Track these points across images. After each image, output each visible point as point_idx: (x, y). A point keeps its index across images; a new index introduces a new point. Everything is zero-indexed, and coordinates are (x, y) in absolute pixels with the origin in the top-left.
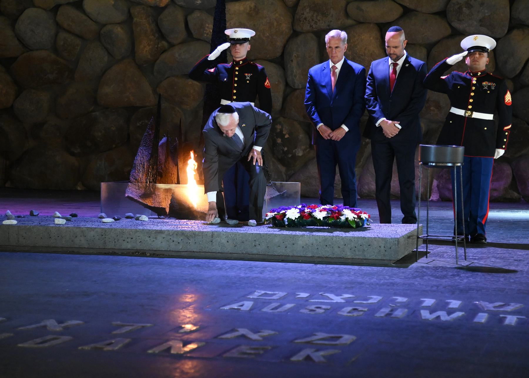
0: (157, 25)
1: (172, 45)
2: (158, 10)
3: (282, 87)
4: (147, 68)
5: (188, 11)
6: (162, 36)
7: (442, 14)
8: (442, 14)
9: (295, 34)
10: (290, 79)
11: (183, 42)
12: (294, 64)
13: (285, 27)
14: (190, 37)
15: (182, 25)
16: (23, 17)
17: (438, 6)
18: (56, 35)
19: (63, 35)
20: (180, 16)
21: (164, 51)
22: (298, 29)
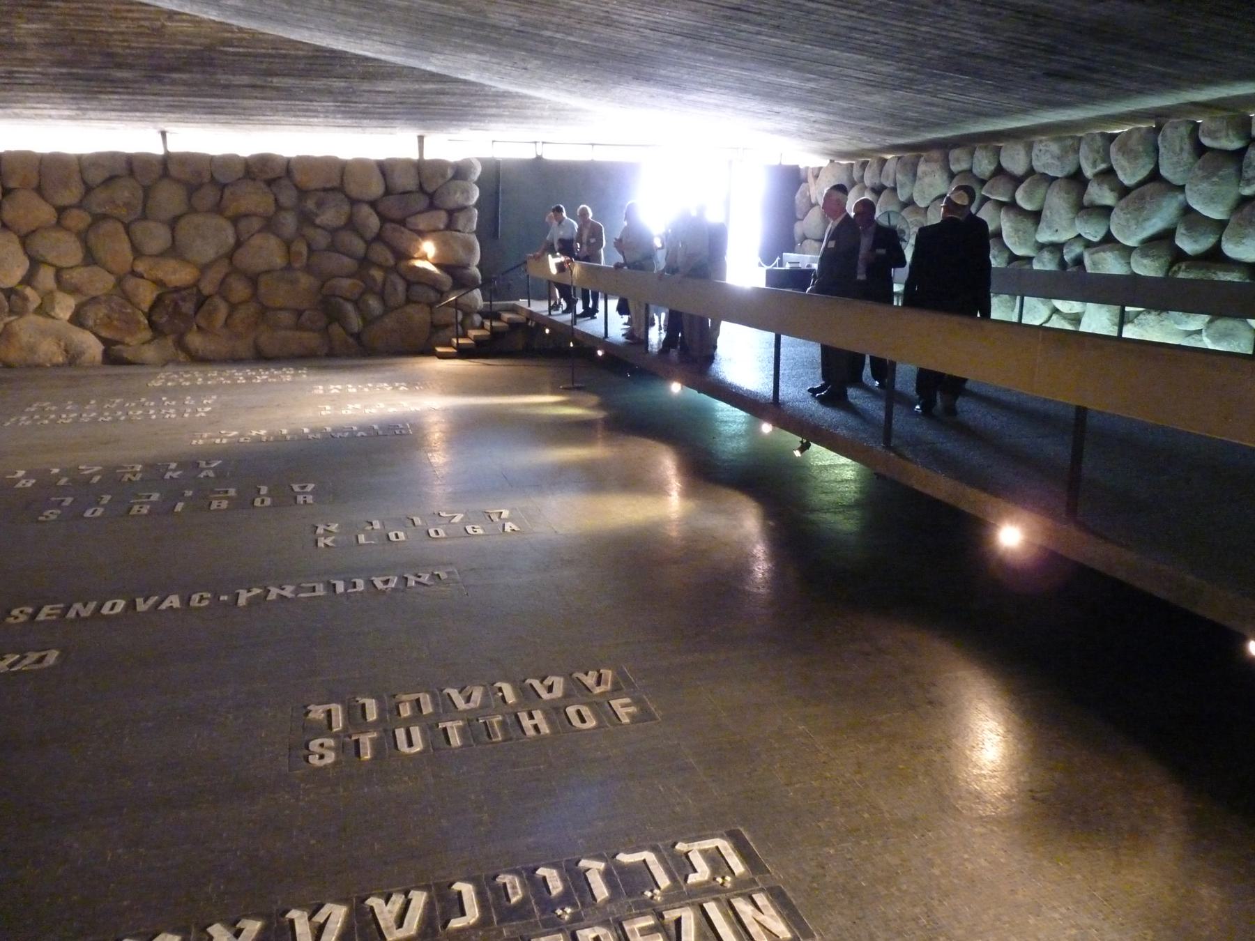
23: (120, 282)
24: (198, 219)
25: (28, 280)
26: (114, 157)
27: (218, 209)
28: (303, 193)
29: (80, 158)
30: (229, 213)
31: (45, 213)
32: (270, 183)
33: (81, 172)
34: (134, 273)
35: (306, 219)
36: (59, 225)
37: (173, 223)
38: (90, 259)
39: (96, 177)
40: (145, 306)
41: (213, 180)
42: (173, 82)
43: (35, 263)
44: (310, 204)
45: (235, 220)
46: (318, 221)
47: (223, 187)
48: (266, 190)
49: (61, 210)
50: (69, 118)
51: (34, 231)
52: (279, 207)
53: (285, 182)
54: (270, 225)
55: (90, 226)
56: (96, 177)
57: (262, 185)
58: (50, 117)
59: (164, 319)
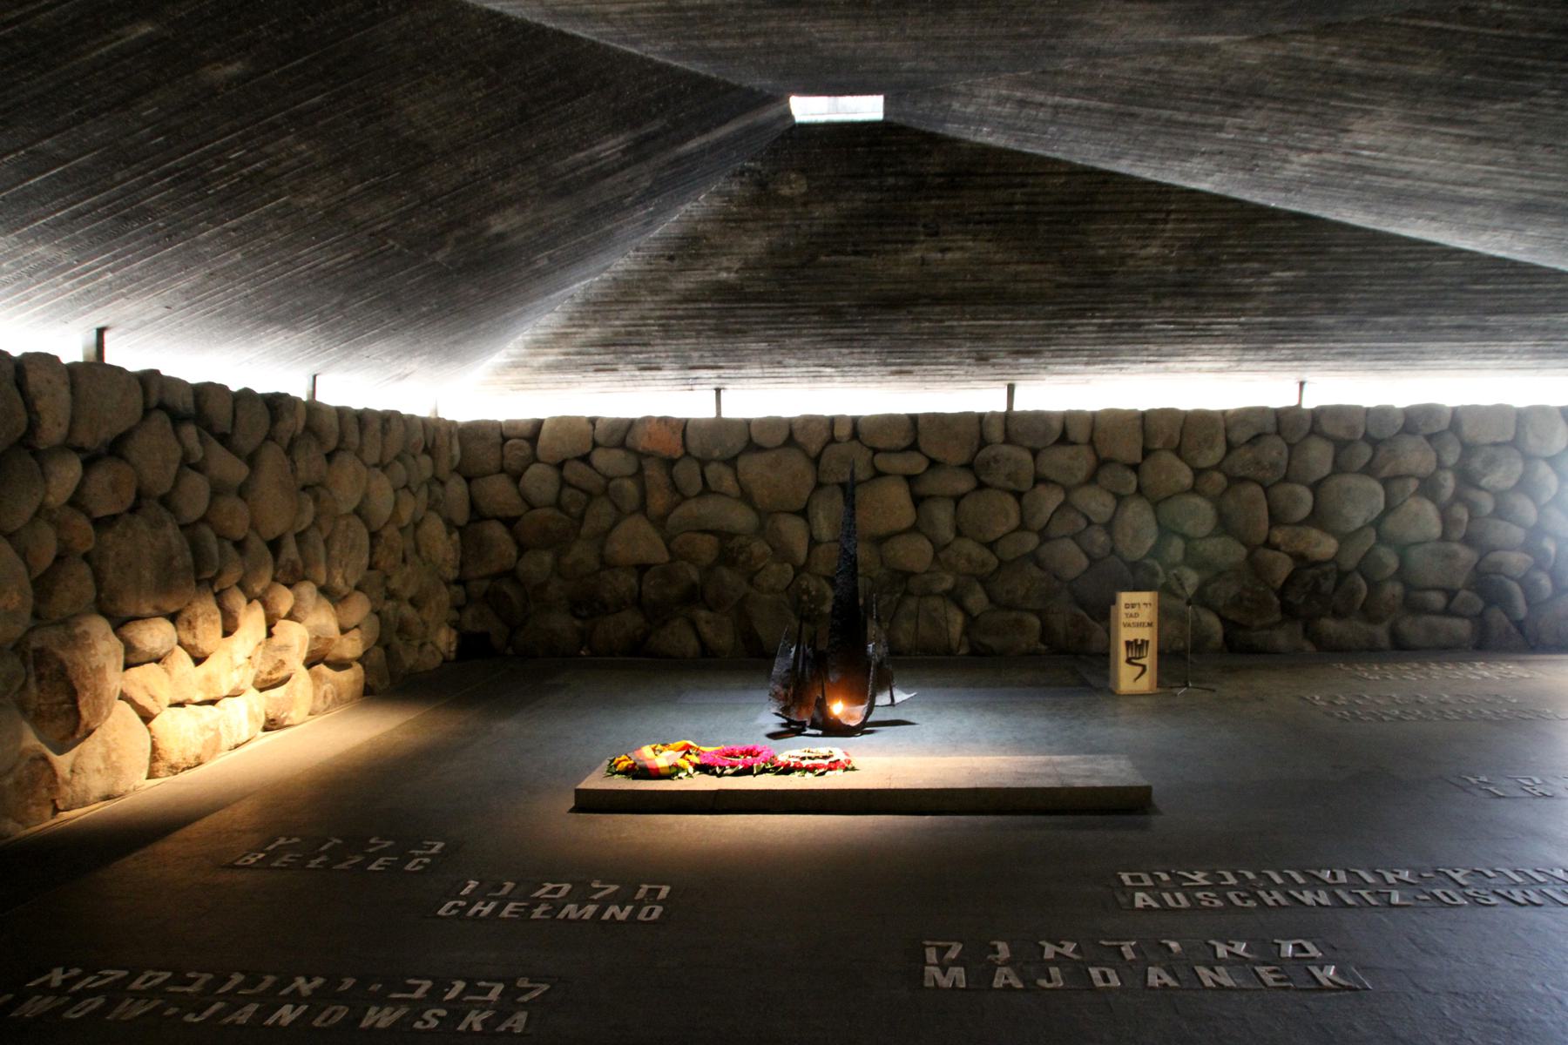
0: (671, 477)
1: (685, 498)
2: (670, 463)
3: (806, 540)
4: (660, 522)
5: (703, 463)
6: (674, 487)
7: (969, 466)
8: (969, 466)
9: (819, 485)
10: (815, 533)
11: (700, 495)
12: (821, 515)
13: (810, 480)
14: (706, 490)
15: (699, 479)
16: (528, 473)
17: (964, 457)
18: (560, 492)
19: (568, 492)
20: (696, 468)
21: (678, 504)
22: (824, 479)
23: (1252, 549)
24: (1351, 481)
25: (1155, 552)
26: (1262, 411)
27: (1369, 470)
28: (1468, 449)
29: (1224, 413)
30: (1385, 472)
31: (1185, 477)
32: (1430, 438)
33: (1226, 430)
34: (1269, 544)
35: (1466, 478)
36: (1194, 490)
37: (1316, 487)
38: (1224, 525)
39: (1240, 435)
40: (1280, 582)
41: (1367, 437)
42: (1376, 326)
43: (1165, 531)
44: (1476, 464)
45: (1386, 482)
46: (1483, 482)
47: (1374, 443)
48: (1427, 446)
49: (1198, 472)
50: (1221, 371)
51: (1169, 498)
52: (1440, 465)
53: (1450, 436)
54: (1428, 487)
55: (1226, 490)
56: (1240, 435)
57: (1421, 439)
58: (1199, 370)
59: (1300, 601)
